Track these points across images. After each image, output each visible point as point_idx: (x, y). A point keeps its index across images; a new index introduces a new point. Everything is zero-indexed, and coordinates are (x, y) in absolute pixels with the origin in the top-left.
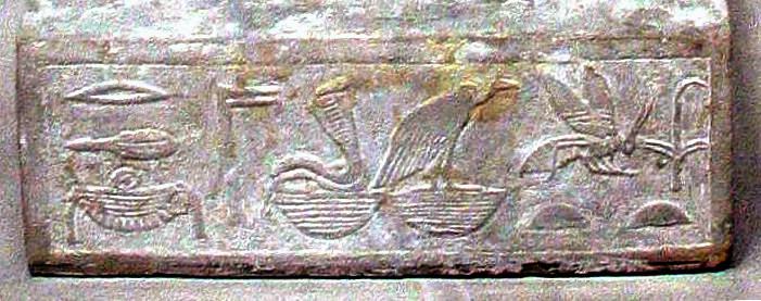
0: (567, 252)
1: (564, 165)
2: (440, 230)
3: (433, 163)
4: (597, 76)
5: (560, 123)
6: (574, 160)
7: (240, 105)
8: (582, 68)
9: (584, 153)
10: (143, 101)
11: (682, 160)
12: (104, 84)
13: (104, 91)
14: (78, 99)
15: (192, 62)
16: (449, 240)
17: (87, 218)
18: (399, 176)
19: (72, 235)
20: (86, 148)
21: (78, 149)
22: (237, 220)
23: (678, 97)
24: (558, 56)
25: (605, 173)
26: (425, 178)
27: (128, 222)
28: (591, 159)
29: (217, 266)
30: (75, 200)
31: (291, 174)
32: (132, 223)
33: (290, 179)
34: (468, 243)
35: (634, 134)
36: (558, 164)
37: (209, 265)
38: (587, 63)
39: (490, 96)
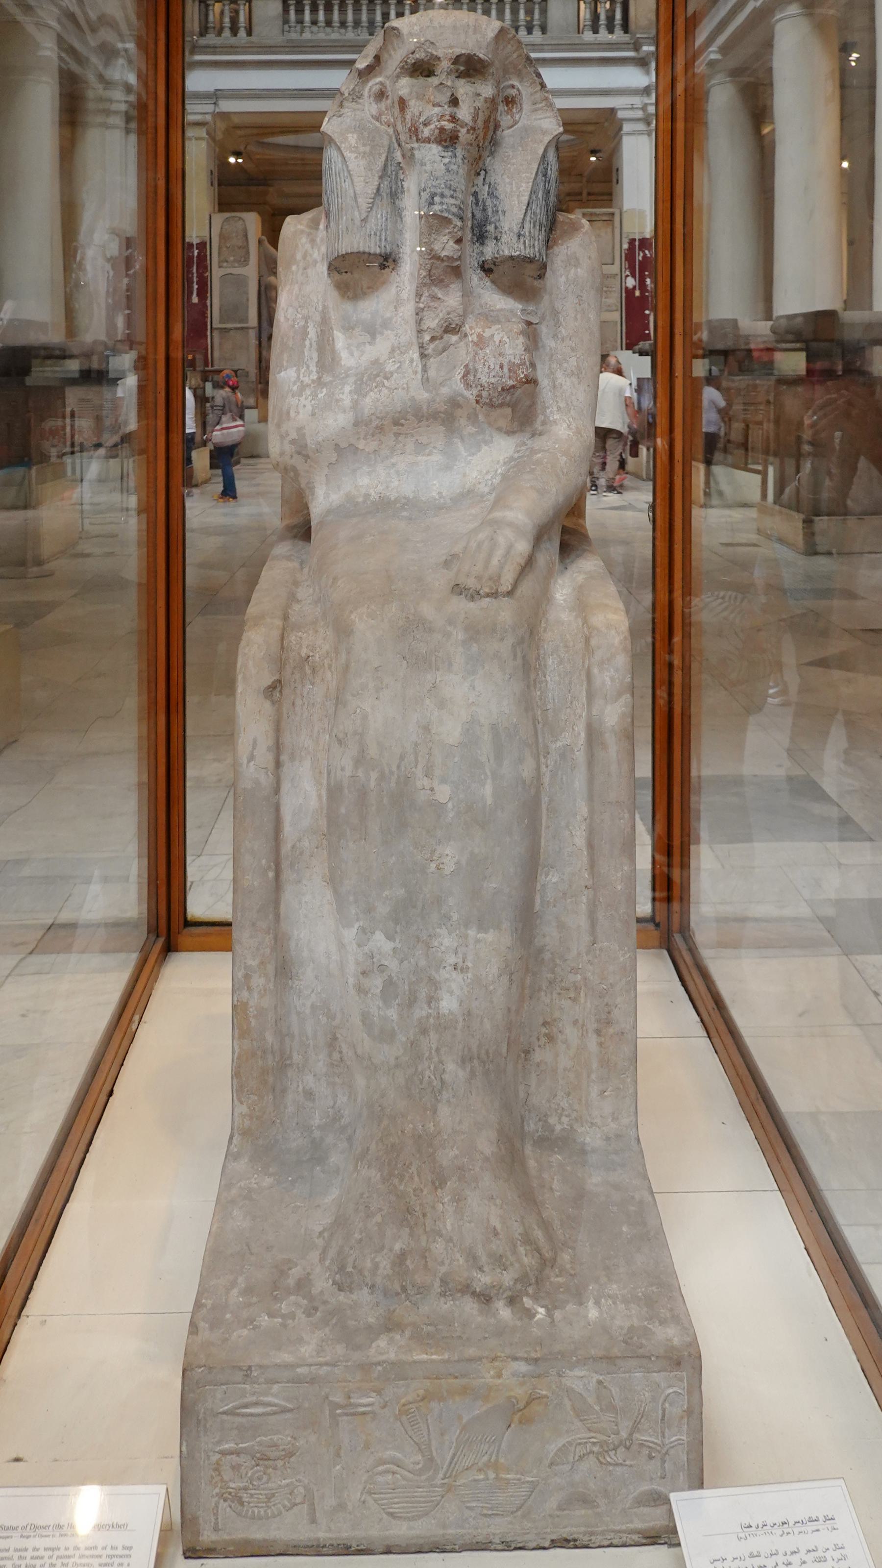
0: (583, 1529)
1: (581, 1458)
2: (490, 1512)
3: (485, 1458)
4: (605, 1387)
5: (579, 1424)
6: (588, 1454)
7: (346, 1414)
8: (594, 1380)
9: (596, 1449)
10: (275, 1413)
11: (666, 1453)
12: (246, 1400)
13: (246, 1406)
14: (224, 1413)
15: (313, 1380)
16: (498, 1520)
17: (228, 1509)
18: (461, 1469)
19: (216, 1524)
20: (231, 1453)
21: (223, 1453)
22: (341, 1506)
23: (663, 1404)
24: (578, 1372)
25: (609, 1464)
26: (480, 1470)
27: (259, 1512)
28: (599, 1453)
29: (324, 1546)
30: (221, 1496)
31: (381, 1468)
32: (262, 1513)
33: (380, 1474)
34: (511, 1523)
35: (631, 1434)
36: (577, 1458)
37: (318, 1546)
38: (596, 1377)
39: (528, 1404)
